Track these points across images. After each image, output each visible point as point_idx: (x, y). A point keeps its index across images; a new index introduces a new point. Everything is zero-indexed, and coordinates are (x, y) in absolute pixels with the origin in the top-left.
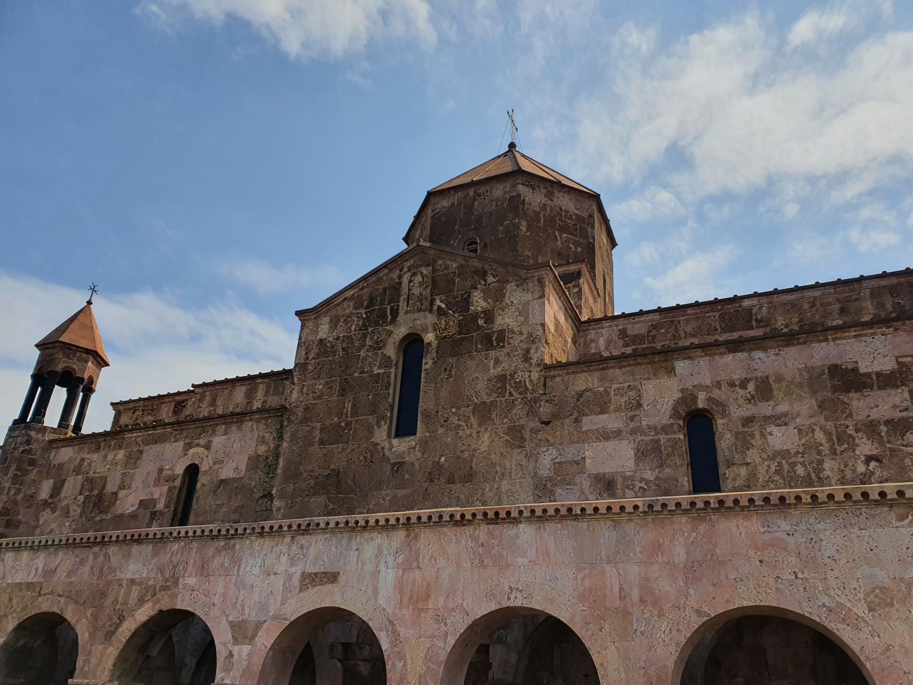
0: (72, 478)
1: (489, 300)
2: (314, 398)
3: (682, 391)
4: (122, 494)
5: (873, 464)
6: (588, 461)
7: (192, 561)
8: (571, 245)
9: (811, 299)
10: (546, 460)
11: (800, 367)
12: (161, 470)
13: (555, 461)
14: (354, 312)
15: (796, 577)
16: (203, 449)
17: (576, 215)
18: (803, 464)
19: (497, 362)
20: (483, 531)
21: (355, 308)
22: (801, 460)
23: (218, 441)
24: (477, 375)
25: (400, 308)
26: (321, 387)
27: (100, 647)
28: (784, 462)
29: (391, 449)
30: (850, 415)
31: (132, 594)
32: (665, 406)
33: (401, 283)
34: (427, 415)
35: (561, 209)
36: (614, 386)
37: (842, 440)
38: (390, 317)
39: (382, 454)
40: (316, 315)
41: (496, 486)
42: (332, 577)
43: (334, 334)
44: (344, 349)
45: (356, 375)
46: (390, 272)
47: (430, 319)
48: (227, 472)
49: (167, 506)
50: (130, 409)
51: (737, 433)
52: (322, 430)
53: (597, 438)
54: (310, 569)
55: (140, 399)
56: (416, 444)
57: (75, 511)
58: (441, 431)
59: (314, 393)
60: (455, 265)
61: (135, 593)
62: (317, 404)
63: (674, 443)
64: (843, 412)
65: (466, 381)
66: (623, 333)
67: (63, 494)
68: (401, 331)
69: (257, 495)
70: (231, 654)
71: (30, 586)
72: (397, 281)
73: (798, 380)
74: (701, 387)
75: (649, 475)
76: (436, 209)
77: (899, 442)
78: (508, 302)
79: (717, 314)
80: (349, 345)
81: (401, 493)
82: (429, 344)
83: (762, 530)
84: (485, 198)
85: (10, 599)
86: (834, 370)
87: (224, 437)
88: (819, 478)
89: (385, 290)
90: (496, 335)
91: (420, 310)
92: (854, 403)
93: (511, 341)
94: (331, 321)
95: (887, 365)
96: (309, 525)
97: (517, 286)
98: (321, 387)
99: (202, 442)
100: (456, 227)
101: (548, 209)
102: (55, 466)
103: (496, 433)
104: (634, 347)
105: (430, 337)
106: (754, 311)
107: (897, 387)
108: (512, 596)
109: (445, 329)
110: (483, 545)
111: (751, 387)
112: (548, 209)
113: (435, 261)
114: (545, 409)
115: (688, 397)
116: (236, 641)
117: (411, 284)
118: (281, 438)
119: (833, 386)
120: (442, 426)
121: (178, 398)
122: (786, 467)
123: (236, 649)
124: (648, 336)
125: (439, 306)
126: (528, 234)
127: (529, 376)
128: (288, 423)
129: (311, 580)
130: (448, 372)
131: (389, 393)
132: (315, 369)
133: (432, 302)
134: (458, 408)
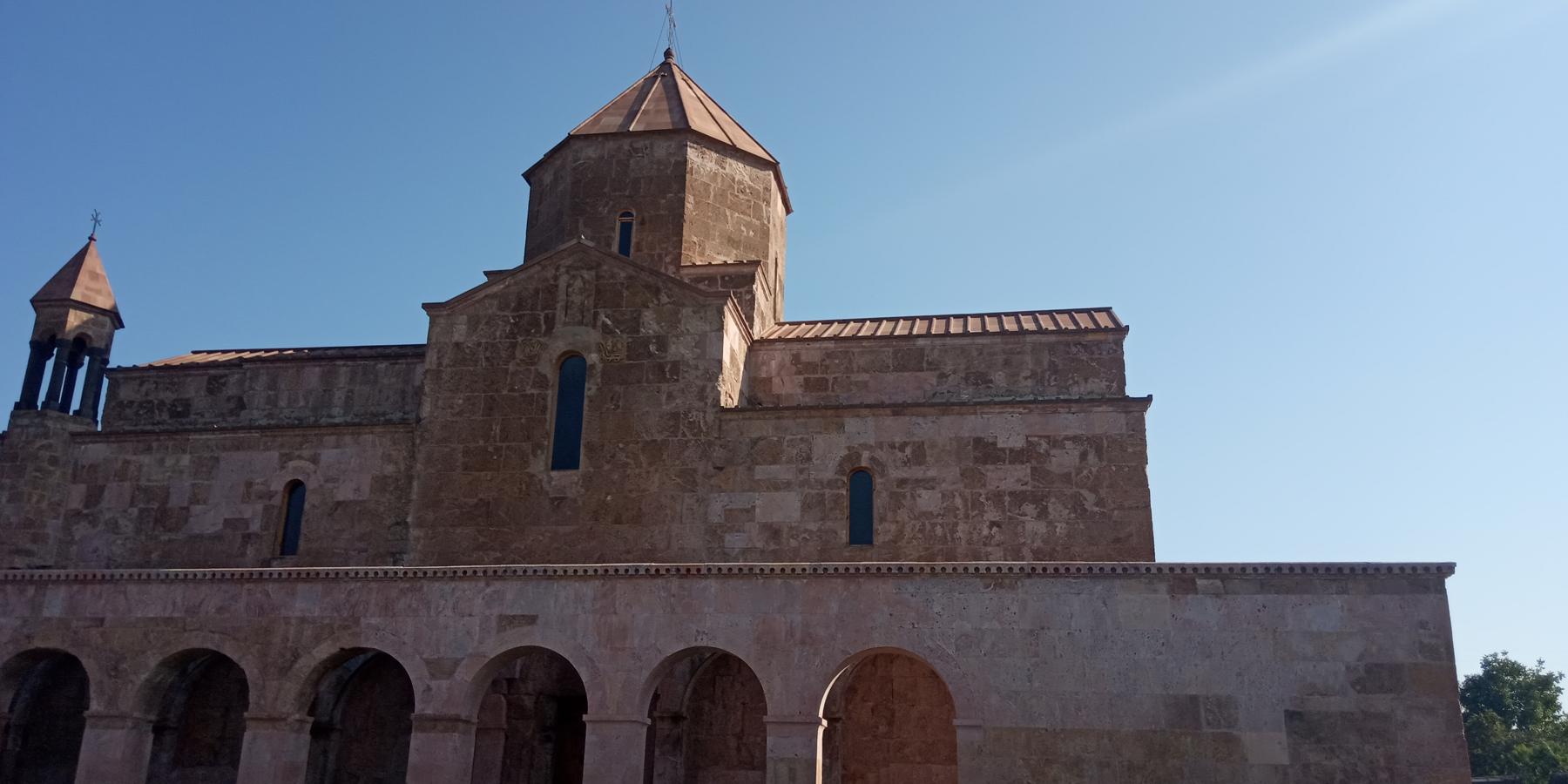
0: (115, 484)
1: (663, 324)
2: (453, 415)
3: (849, 448)
4: (197, 509)
5: (995, 529)
6: (757, 510)
7: (373, 601)
8: (743, 228)
9: (980, 347)
10: (717, 507)
11: (951, 436)
12: (249, 484)
13: (727, 507)
14: (498, 313)
15: (914, 627)
16: (308, 463)
17: (750, 187)
18: (942, 525)
19: (670, 396)
20: (675, 584)
21: (500, 309)
22: (941, 521)
23: (328, 455)
24: (647, 409)
25: (557, 317)
26: (461, 401)
27: (275, 683)
28: (927, 522)
29: (549, 483)
30: (984, 485)
31: (305, 633)
32: (832, 462)
33: (557, 286)
34: (591, 448)
35: (733, 180)
36: (788, 438)
37: (976, 504)
38: (544, 327)
39: (539, 487)
40: (449, 312)
41: (666, 528)
42: (532, 620)
43: (474, 338)
44: (487, 359)
45: (505, 392)
46: (543, 269)
47: (594, 336)
48: (344, 493)
49: (265, 527)
50: (135, 379)
51: (892, 493)
52: (466, 453)
53: (768, 488)
54: (509, 612)
55: (151, 367)
56: (579, 480)
57: (127, 527)
58: (607, 467)
59: (452, 408)
60: (623, 275)
61: (308, 632)
62: (457, 422)
63: (837, 499)
64: (979, 481)
65: (635, 414)
66: (796, 358)
67: (104, 505)
68: (559, 346)
69: (388, 522)
70: (429, 689)
71: (169, 620)
72: (552, 282)
73: (948, 448)
74: (866, 446)
75: (813, 526)
76: (579, 159)
77: (1017, 512)
78: (683, 329)
79: (891, 350)
80: (494, 355)
81: (562, 530)
82: (593, 366)
83: (894, 591)
84: (643, 157)
85: (146, 635)
86: (978, 441)
87: (335, 450)
88: (953, 539)
89: (537, 291)
90: (669, 366)
91: (581, 323)
92: (989, 474)
93: (686, 375)
94: (469, 321)
95: (1018, 443)
96: (505, 571)
97: (694, 312)
98: (461, 401)
99: (306, 453)
100: (606, 190)
101: (719, 180)
102: (83, 467)
103: (667, 474)
104: (806, 376)
105: (593, 358)
106: (927, 352)
107: (1023, 464)
108: (699, 638)
109: (613, 352)
110: (674, 596)
111: (908, 451)
112: (719, 180)
113: (599, 265)
114: (718, 454)
115: (853, 455)
116: (433, 676)
117: (570, 290)
118: (413, 457)
119: (975, 458)
120: (608, 462)
121: (212, 372)
122: (928, 527)
123: (433, 684)
124: (821, 365)
125: (603, 322)
126: (694, 214)
127: (704, 417)
128: (422, 440)
129: (507, 621)
130: (614, 402)
131: (545, 419)
132: (452, 379)
133: (596, 315)
134: (627, 444)
